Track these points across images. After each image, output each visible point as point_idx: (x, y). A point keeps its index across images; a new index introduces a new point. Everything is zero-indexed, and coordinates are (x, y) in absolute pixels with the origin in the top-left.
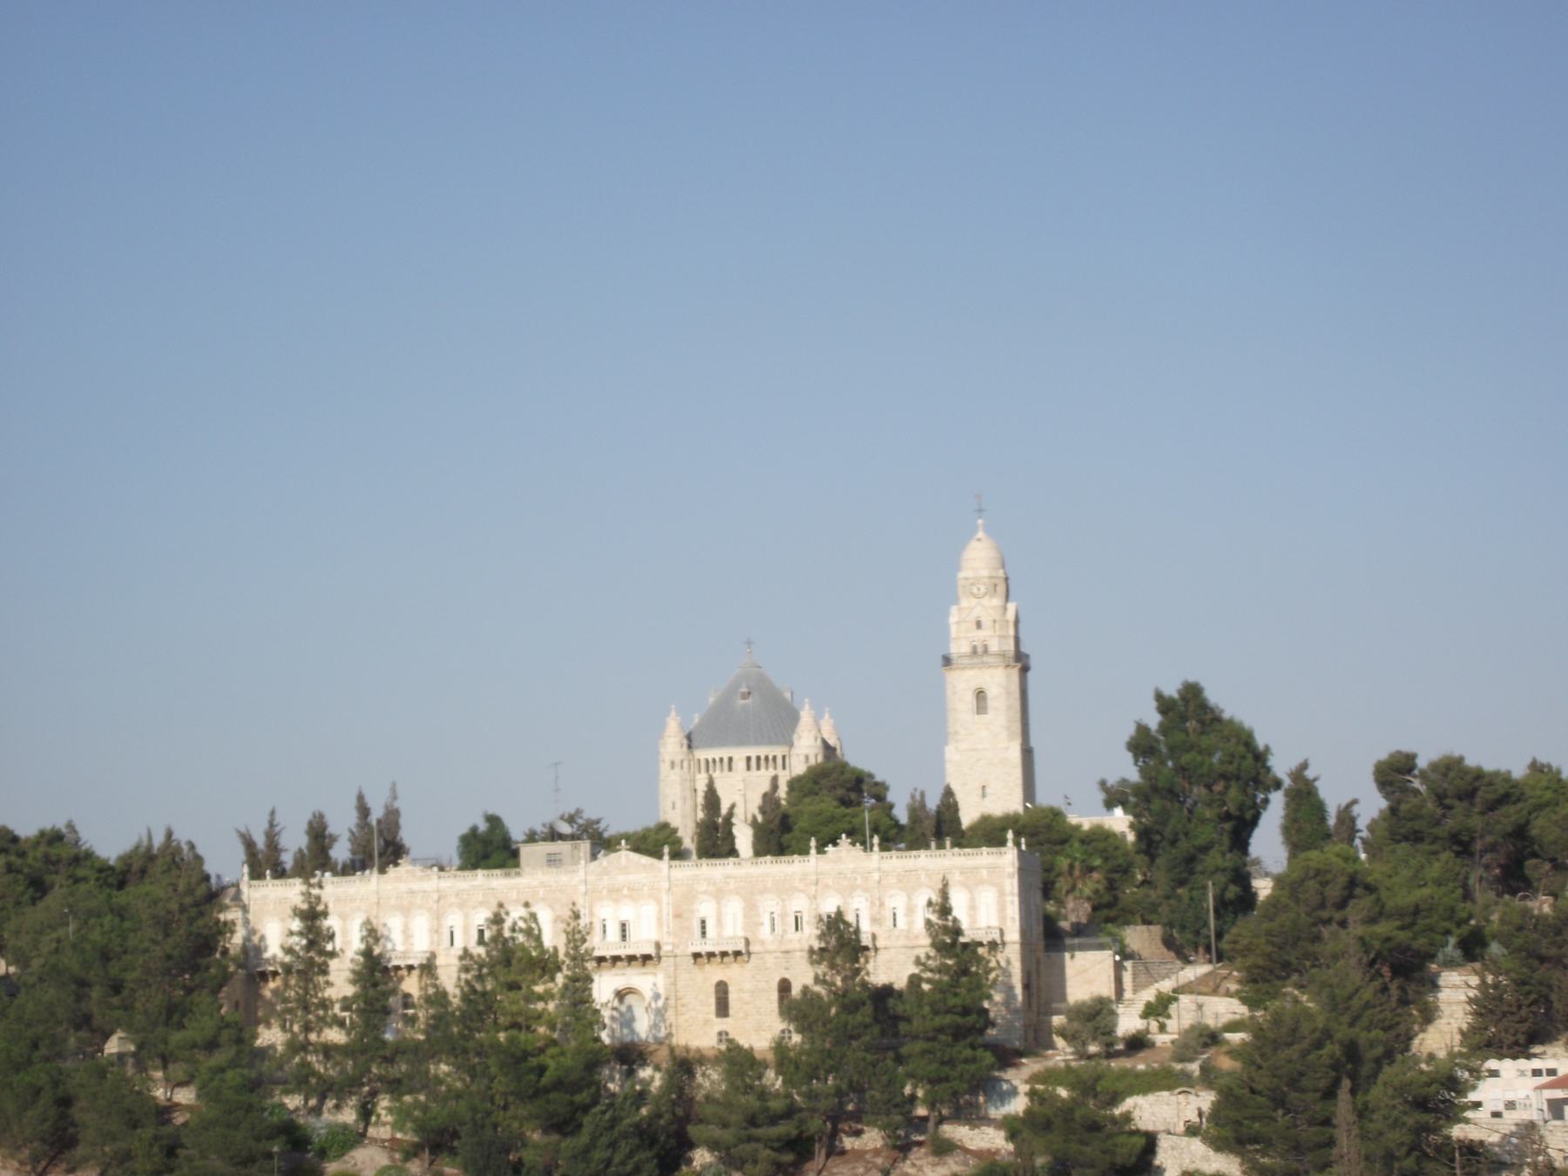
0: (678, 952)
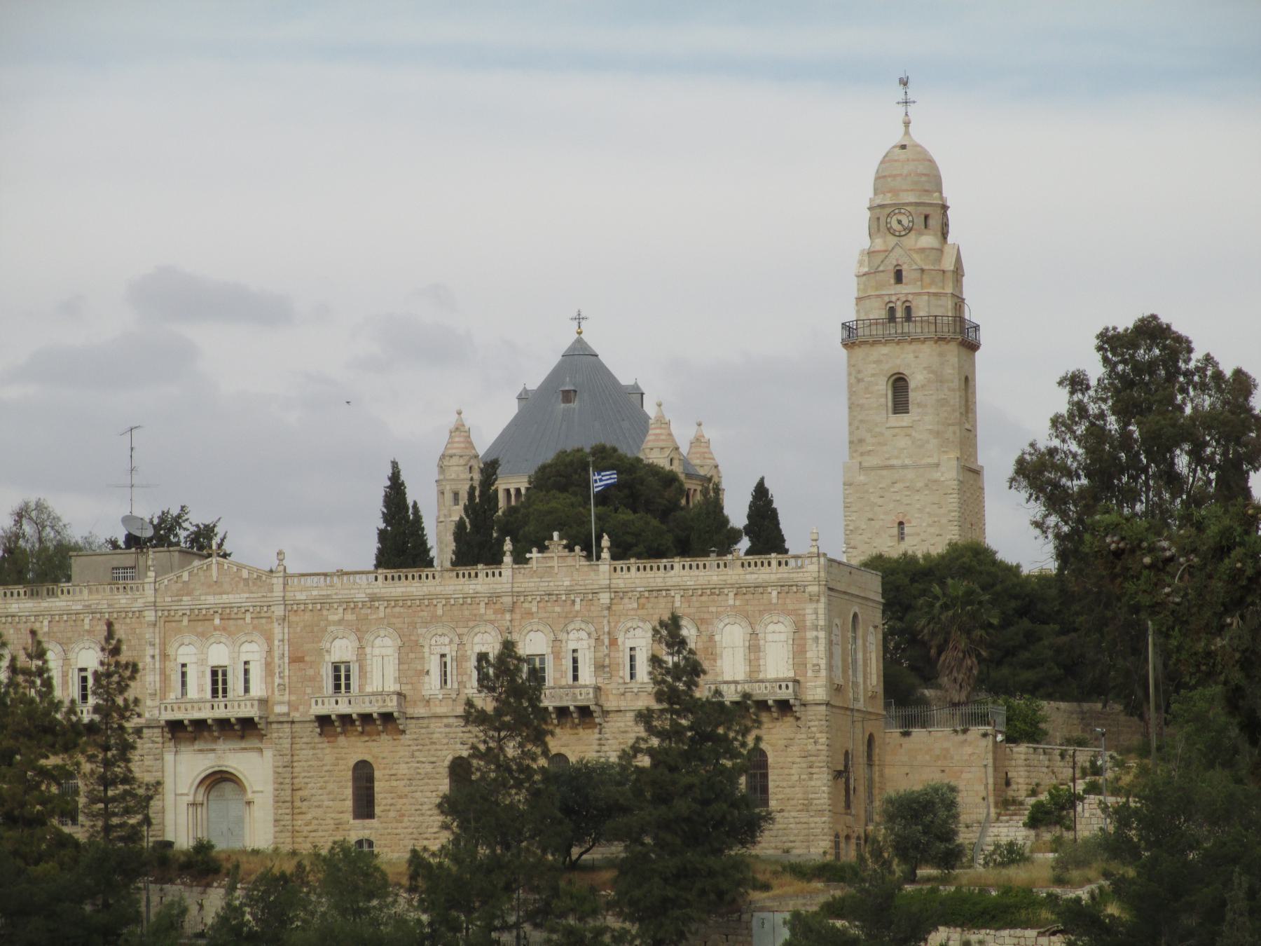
0: (296, 715)
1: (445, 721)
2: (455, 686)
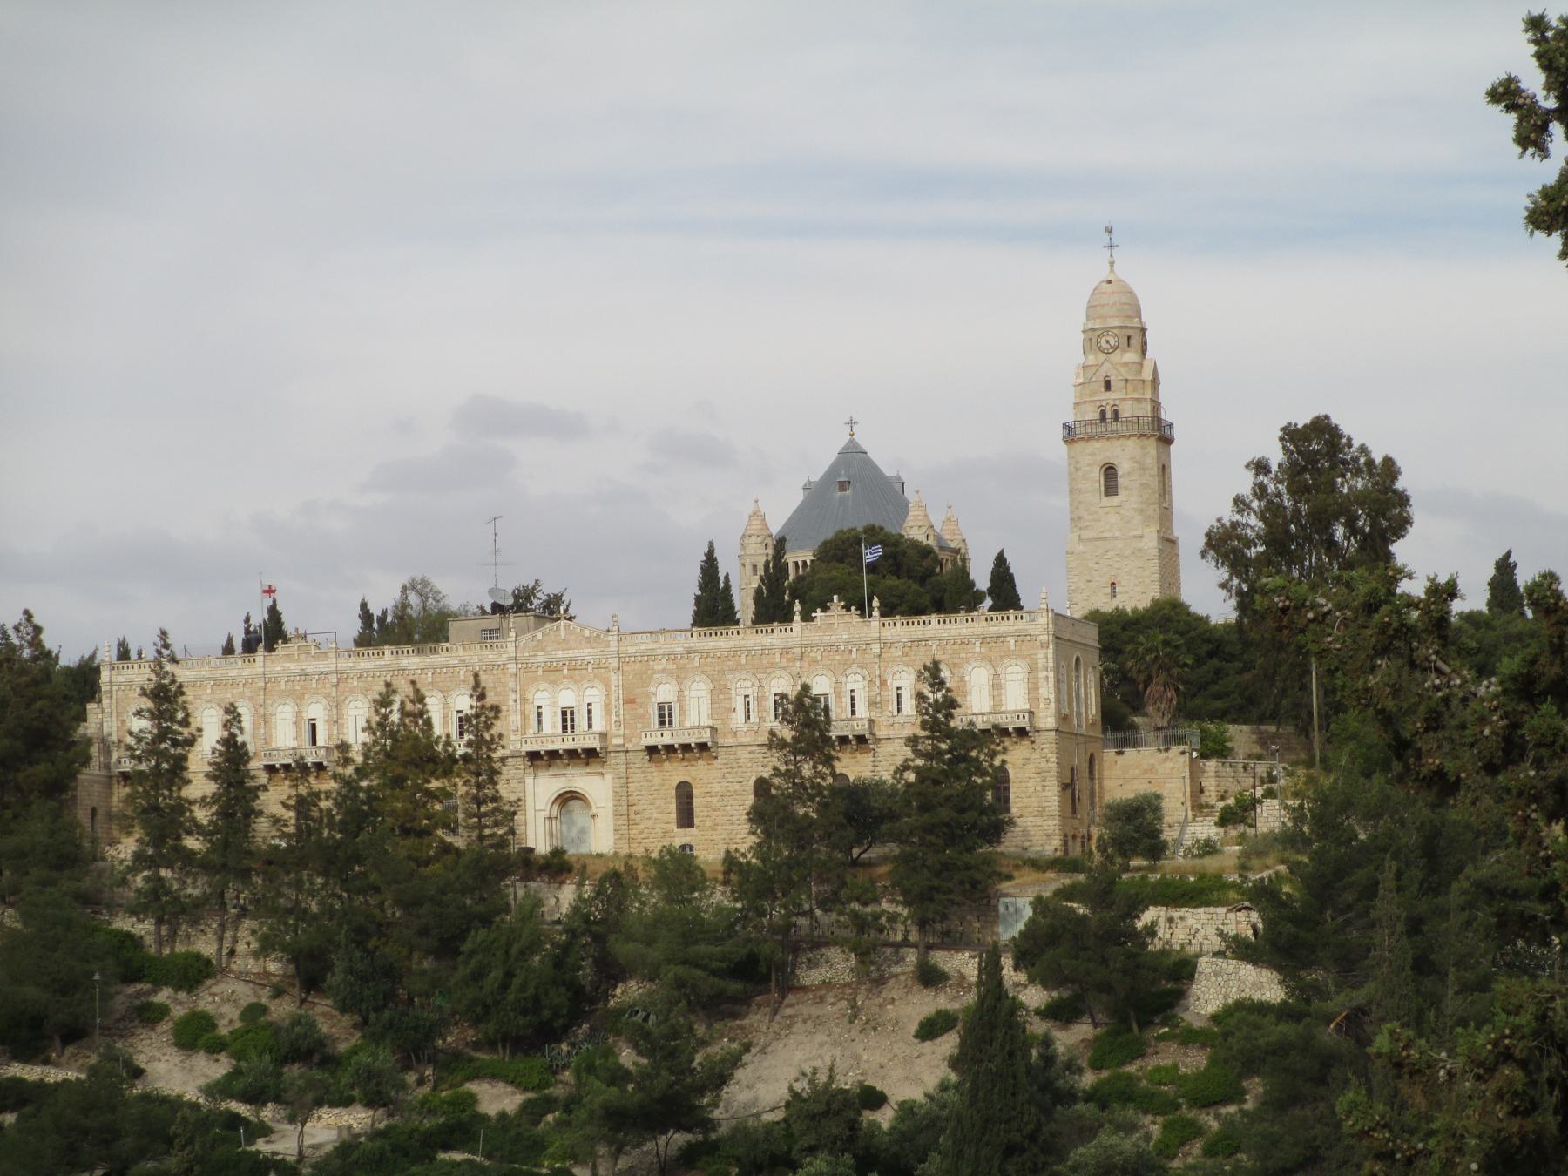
0: (629, 746)
1: (750, 748)
2: (757, 720)
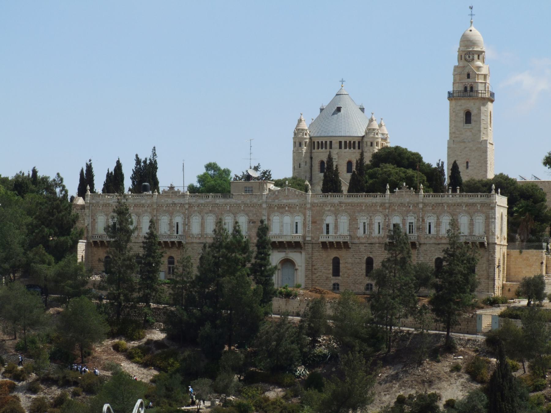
1: (365, 245)
2: (369, 233)
